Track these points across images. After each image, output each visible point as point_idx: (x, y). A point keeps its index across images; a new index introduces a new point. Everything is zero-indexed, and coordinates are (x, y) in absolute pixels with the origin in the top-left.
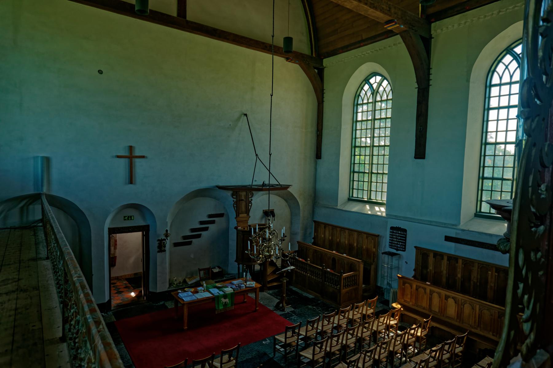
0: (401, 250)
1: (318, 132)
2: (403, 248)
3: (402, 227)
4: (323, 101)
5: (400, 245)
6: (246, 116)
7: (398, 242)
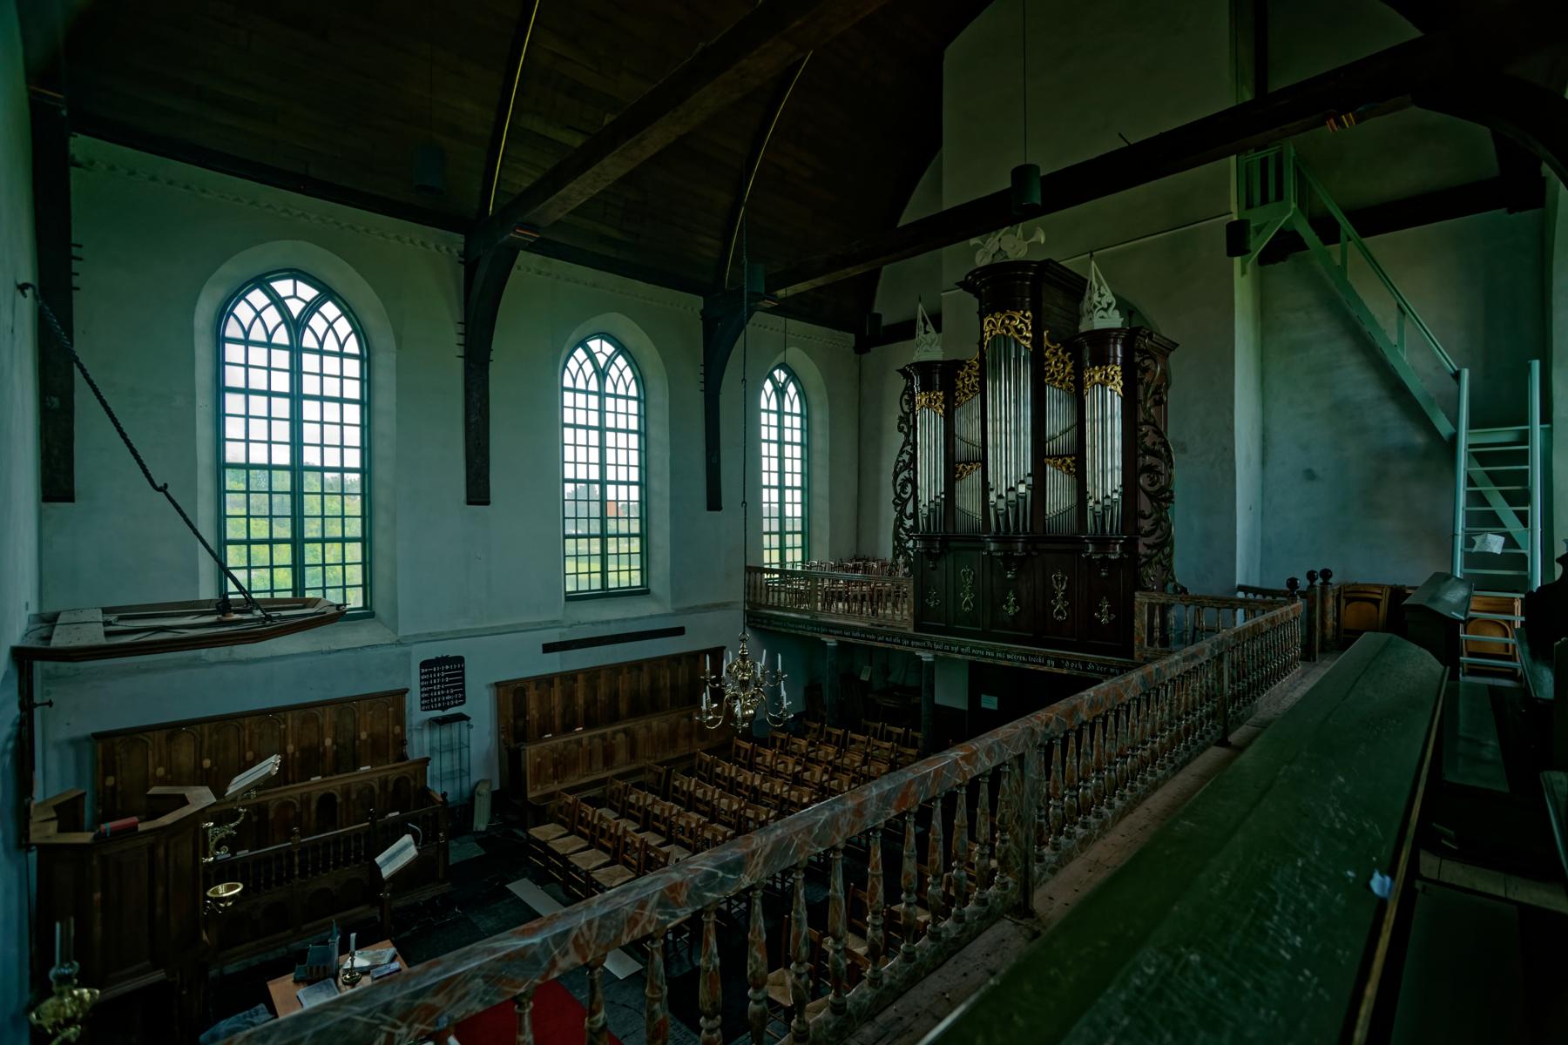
0: (455, 705)
2: (458, 699)
3: (452, 655)
5: (450, 694)
7: (445, 689)
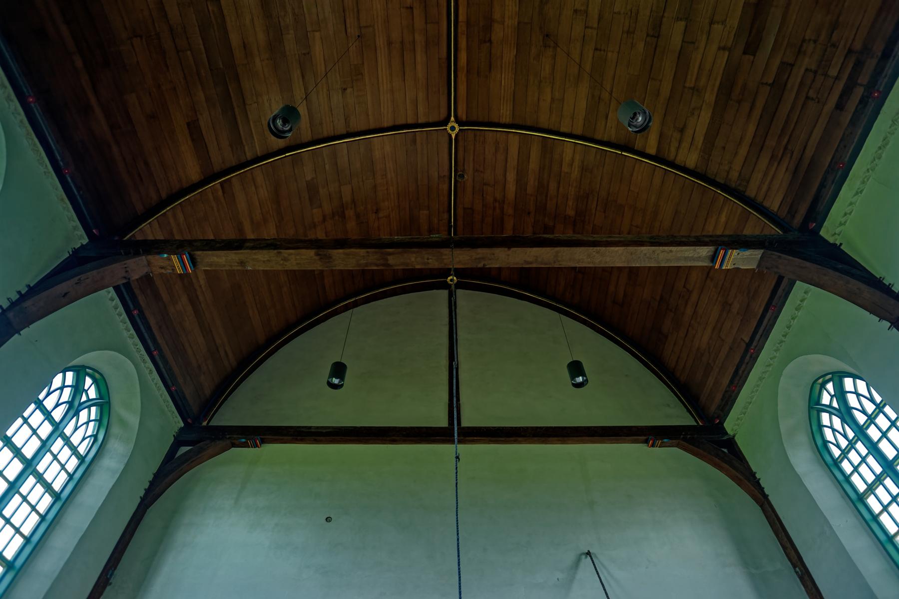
1: (797, 569)
4: (766, 497)
6: (591, 557)
